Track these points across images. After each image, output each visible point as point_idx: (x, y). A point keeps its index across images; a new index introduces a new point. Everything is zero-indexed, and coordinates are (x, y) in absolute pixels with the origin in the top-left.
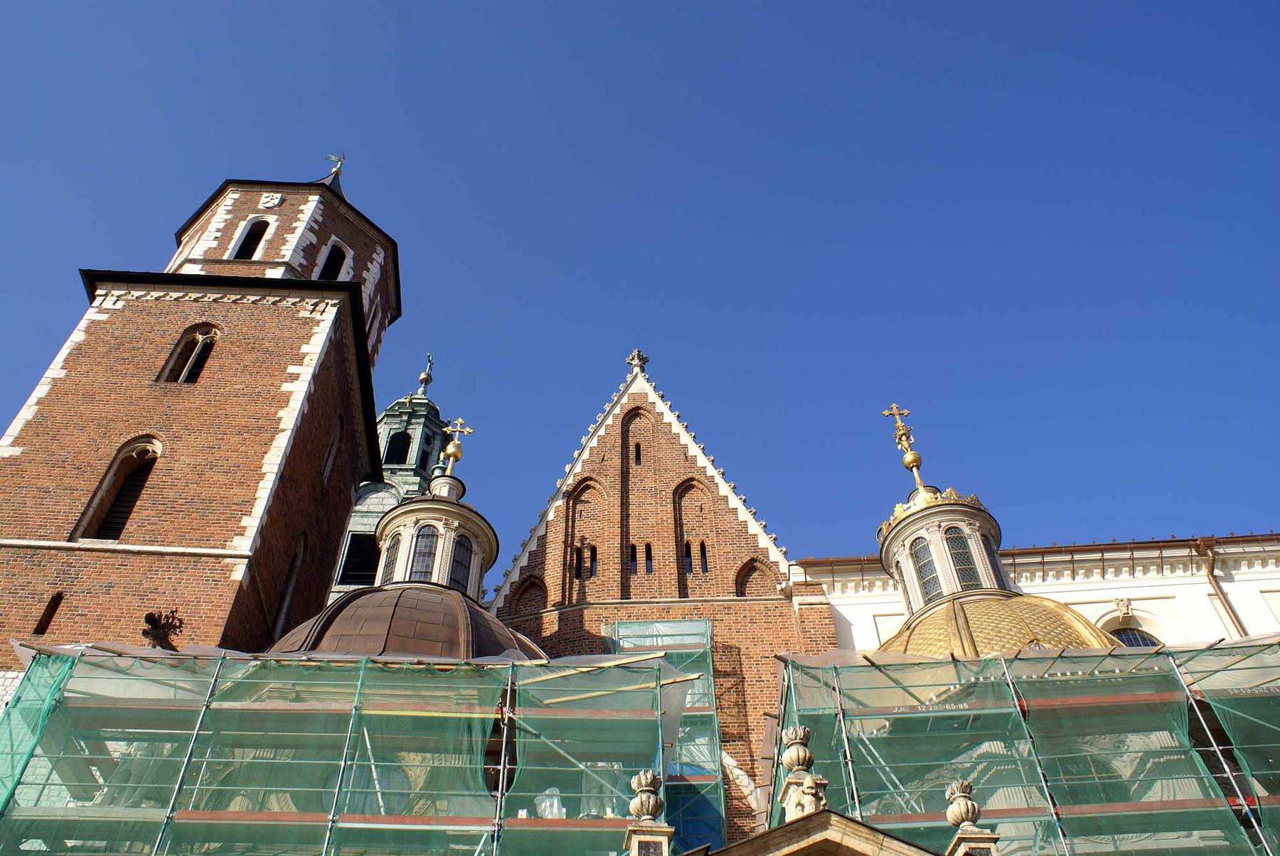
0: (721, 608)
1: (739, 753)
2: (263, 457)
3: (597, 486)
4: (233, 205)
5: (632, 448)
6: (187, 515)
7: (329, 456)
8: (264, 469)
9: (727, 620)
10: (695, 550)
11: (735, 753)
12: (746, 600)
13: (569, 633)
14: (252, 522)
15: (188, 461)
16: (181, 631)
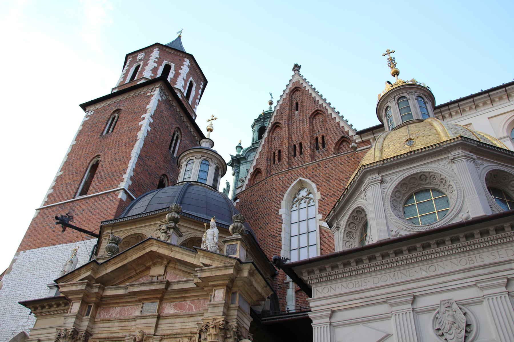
0: (329, 162)
2: (131, 151)
3: (280, 125)
4: (130, 63)
5: (294, 105)
10: (320, 139)
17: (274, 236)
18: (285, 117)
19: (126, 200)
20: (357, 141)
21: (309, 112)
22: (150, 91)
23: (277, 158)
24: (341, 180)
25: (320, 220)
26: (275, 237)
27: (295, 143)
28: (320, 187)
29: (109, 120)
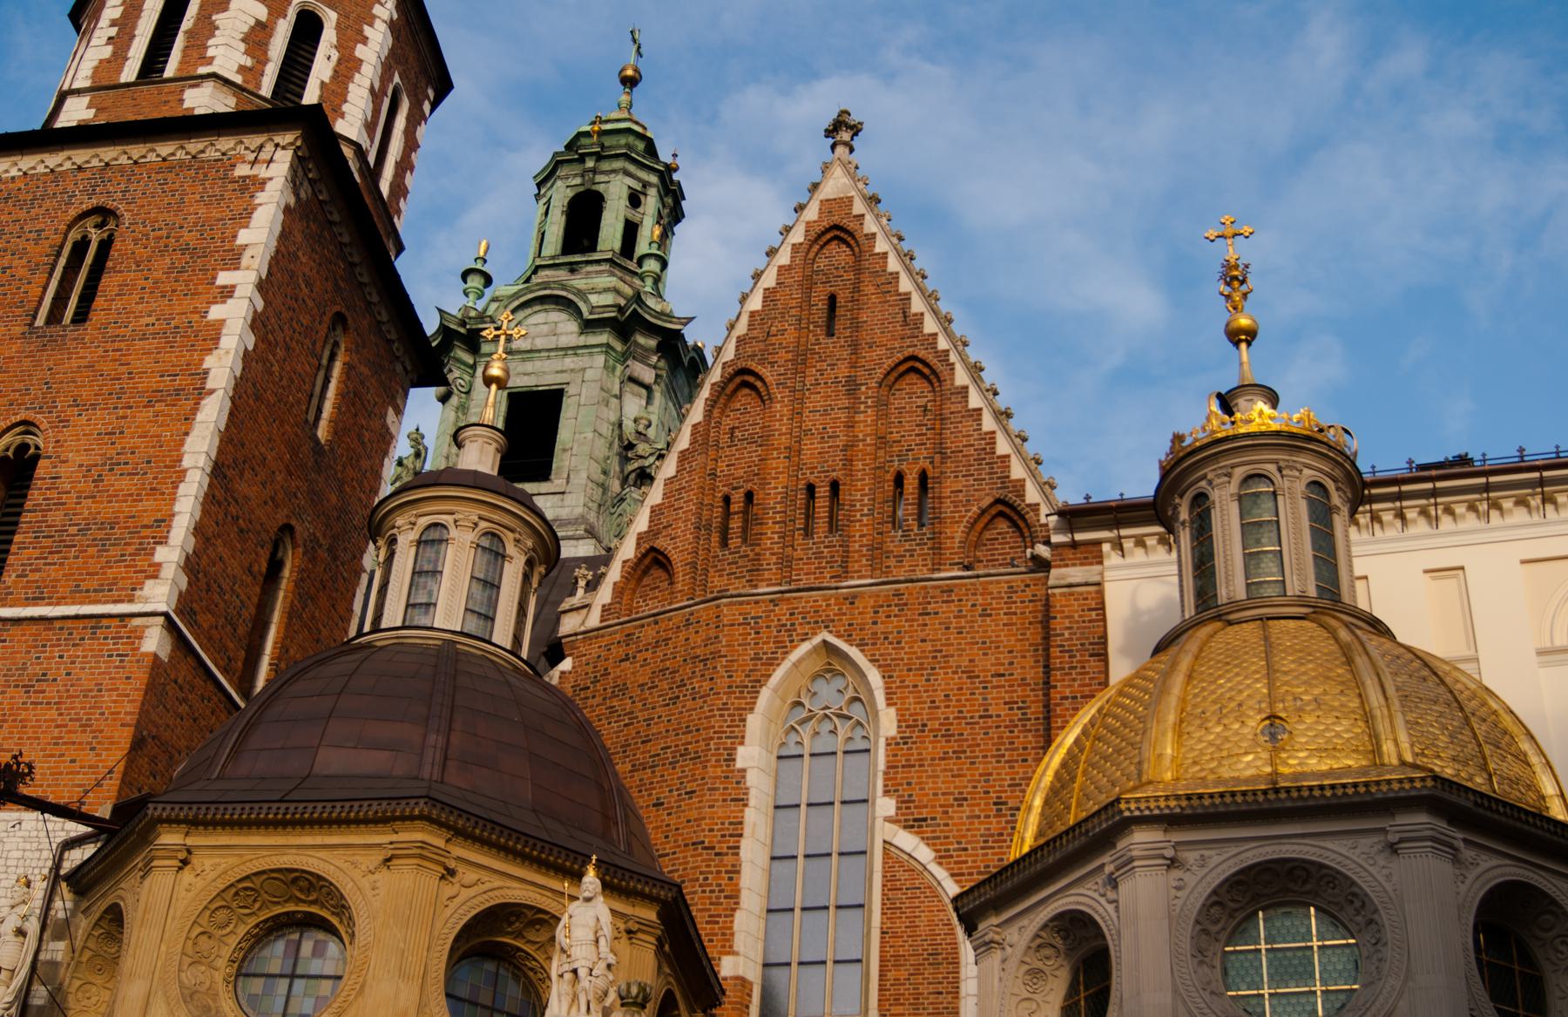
0: (937, 592)
1: (939, 838)
2: (182, 445)
3: (759, 384)
5: (821, 305)
6: (81, 552)
7: (327, 381)
8: (186, 463)
9: (944, 612)
10: (911, 484)
11: (934, 838)
12: (978, 576)
13: (699, 647)
14: (171, 555)
15: (78, 459)
16: (32, 780)
17: (713, 848)
18: (783, 356)
19: (171, 658)
20: (1055, 539)
21: (880, 358)
22: (251, 157)
23: (736, 524)
24: (978, 677)
25: (888, 820)
26: (717, 854)
27: (812, 478)
28: (897, 687)
29: (59, 254)
